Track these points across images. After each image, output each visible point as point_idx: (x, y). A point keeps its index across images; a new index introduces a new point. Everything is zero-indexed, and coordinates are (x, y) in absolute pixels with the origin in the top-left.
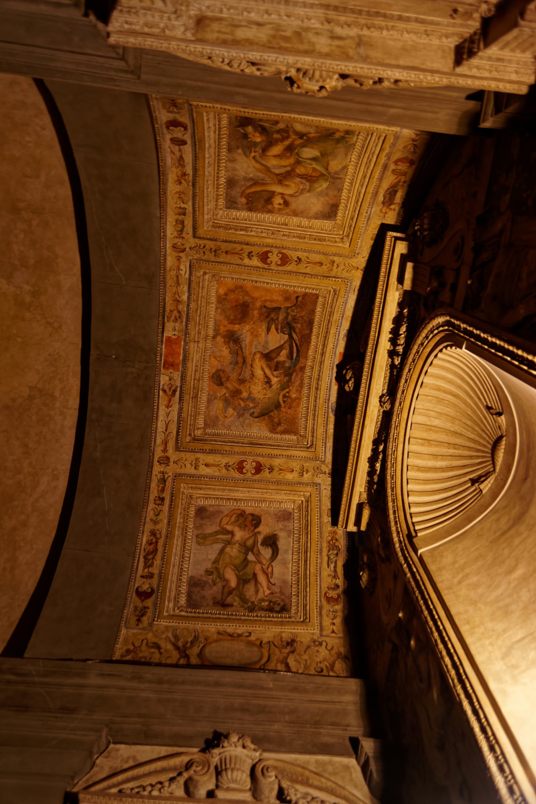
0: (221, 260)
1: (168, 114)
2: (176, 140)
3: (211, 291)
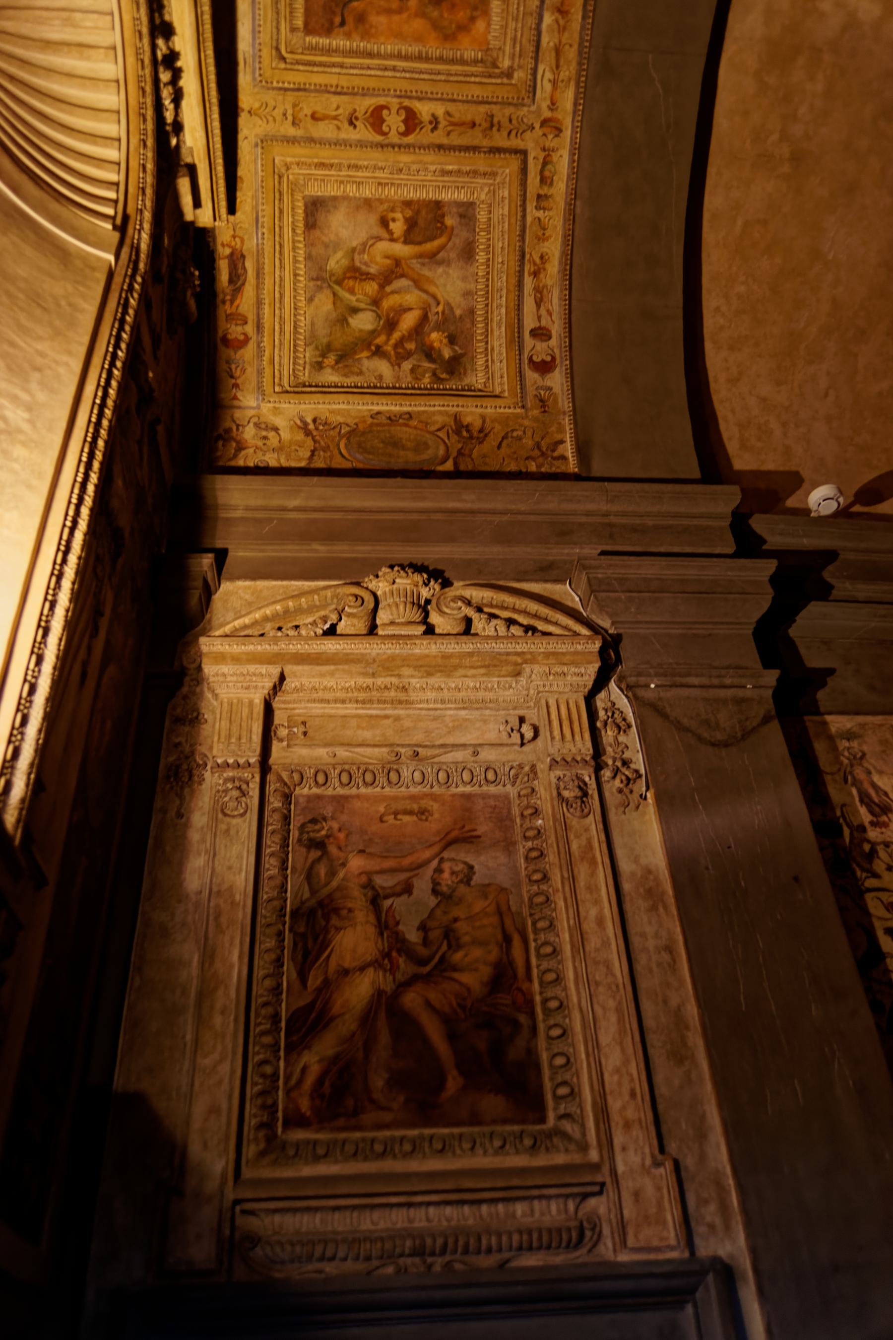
0: (483, 109)
1: (552, 385)
2: (543, 338)
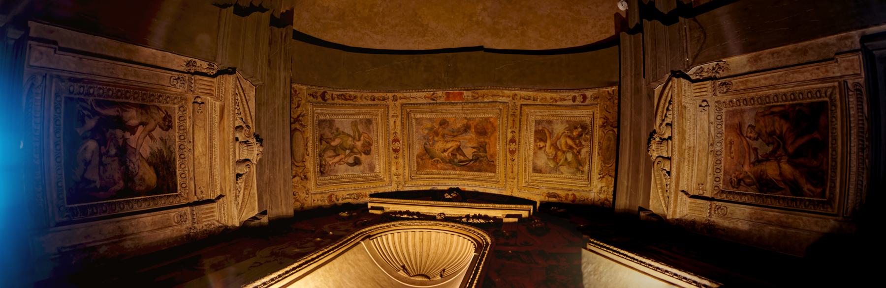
3: (491, 115)
